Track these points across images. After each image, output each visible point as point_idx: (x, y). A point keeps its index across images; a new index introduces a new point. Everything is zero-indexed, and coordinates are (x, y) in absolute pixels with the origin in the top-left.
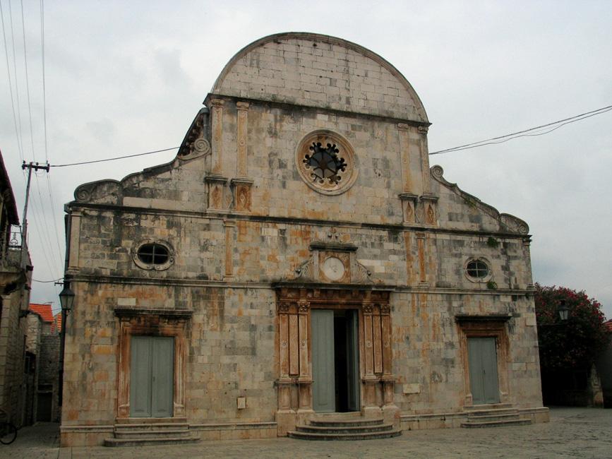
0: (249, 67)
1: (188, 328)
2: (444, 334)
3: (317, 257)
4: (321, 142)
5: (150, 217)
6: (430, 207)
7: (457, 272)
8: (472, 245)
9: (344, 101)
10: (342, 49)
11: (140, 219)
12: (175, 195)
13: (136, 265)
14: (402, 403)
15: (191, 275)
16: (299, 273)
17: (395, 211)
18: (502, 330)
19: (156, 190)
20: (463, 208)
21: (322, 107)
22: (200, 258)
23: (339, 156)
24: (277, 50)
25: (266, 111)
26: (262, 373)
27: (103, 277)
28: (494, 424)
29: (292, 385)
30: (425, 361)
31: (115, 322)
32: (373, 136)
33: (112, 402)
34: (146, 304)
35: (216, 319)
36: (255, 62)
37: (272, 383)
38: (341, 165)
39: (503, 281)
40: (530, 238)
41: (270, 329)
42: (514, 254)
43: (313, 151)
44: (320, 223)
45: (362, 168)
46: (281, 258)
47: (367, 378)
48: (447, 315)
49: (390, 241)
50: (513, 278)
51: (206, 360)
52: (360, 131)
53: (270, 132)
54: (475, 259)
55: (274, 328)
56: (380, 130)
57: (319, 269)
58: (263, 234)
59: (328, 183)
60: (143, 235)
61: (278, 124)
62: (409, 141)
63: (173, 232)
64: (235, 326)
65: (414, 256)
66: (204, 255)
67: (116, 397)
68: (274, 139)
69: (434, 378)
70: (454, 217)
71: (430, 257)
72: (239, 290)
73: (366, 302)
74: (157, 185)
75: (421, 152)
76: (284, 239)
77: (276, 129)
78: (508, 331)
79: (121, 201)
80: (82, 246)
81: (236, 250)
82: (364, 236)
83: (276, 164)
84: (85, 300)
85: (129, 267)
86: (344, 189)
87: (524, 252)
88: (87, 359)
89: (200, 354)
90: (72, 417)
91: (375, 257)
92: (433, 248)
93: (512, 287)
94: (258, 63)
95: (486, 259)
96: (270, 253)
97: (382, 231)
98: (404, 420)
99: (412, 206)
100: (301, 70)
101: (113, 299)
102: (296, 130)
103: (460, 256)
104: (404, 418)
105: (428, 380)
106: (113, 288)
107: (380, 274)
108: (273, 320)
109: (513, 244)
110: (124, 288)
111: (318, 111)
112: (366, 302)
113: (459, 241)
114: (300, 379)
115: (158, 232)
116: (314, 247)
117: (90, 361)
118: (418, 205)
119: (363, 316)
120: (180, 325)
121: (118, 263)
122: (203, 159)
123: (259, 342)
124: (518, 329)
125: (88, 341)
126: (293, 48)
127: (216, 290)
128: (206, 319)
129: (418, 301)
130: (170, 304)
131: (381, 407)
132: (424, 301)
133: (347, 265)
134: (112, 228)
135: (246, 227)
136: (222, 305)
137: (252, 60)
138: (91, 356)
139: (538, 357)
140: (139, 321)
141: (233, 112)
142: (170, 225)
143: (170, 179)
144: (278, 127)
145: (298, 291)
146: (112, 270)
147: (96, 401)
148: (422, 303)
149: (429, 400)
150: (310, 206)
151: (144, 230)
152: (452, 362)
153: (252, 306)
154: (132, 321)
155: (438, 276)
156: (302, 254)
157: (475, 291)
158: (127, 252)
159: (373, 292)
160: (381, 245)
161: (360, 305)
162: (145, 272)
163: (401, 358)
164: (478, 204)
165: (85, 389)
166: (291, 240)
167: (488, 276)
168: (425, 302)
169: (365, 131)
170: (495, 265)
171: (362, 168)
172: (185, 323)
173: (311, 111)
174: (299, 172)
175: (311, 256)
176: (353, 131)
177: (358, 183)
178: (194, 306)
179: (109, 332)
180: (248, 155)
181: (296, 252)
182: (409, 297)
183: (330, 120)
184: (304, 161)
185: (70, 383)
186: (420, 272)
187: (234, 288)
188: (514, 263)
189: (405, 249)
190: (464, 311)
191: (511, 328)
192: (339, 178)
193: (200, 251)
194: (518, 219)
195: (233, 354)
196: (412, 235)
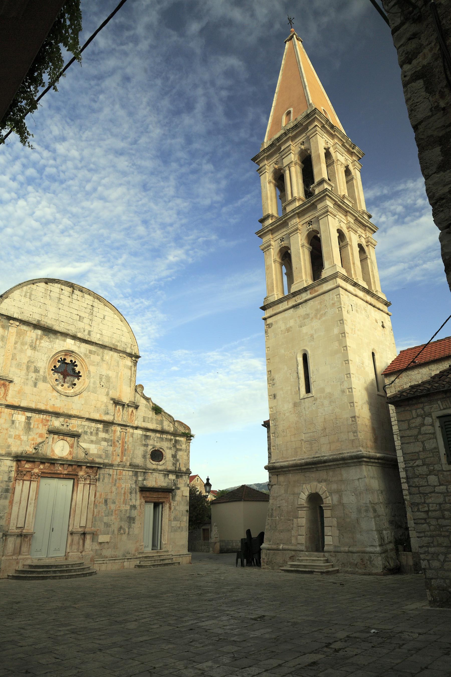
0: (23, 297)
3: (52, 439)
7: (144, 457)
9: (86, 333)
14: (96, 550)
18: (167, 498)
20: (153, 414)
23: (77, 369)
24: (46, 290)
25: (31, 331)
28: (157, 565)
29: (18, 536)
30: (116, 519)
32: (102, 360)
38: (78, 375)
39: (171, 465)
41: (7, 491)
42: (180, 448)
43: (60, 364)
44: (57, 415)
45: (92, 380)
46: (24, 438)
47: (74, 530)
48: (134, 486)
49: (103, 432)
52: (94, 354)
53: (31, 346)
54: (156, 449)
55: (11, 491)
56: (108, 355)
57: (52, 448)
58: (14, 419)
59: (67, 387)
65: (118, 444)
68: (34, 351)
69: (120, 531)
70: (146, 420)
82: (86, 427)
83: (32, 368)
86: (78, 392)
87: (186, 447)
91: (92, 442)
93: (177, 469)
94: (30, 296)
96: (17, 433)
98: (95, 562)
99: (121, 409)
100: (61, 306)
102: (50, 347)
103: (146, 445)
104: (97, 561)
105: (116, 532)
107: (93, 454)
111: (68, 337)
112: (81, 473)
114: (24, 531)
116: (51, 432)
118: (125, 409)
119: (78, 483)
124: (178, 498)
126: (58, 290)
131: (81, 552)
133: (72, 447)
137: (26, 292)
139: (188, 517)
144: (38, 343)
149: (115, 547)
150: (52, 402)
156: (41, 436)
157: (154, 470)
160: (97, 434)
161: (77, 475)
163: (100, 516)
166: (34, 424)
167: (163, 460)
168: (121, 476)
170: (168, 454)
171: (92, 380)
175: (47, 438)
176: (89, 354)
177: (87, 389)
180: (12, 359)
181: (37, 434)
182: (111, 472)
184: (52, 370)
186: (120, 455)
188: (180, 453)
189: (112, 438)
190: (145, 483)
191: (174, 497)
194: (185, 425)
196: (118, 429)
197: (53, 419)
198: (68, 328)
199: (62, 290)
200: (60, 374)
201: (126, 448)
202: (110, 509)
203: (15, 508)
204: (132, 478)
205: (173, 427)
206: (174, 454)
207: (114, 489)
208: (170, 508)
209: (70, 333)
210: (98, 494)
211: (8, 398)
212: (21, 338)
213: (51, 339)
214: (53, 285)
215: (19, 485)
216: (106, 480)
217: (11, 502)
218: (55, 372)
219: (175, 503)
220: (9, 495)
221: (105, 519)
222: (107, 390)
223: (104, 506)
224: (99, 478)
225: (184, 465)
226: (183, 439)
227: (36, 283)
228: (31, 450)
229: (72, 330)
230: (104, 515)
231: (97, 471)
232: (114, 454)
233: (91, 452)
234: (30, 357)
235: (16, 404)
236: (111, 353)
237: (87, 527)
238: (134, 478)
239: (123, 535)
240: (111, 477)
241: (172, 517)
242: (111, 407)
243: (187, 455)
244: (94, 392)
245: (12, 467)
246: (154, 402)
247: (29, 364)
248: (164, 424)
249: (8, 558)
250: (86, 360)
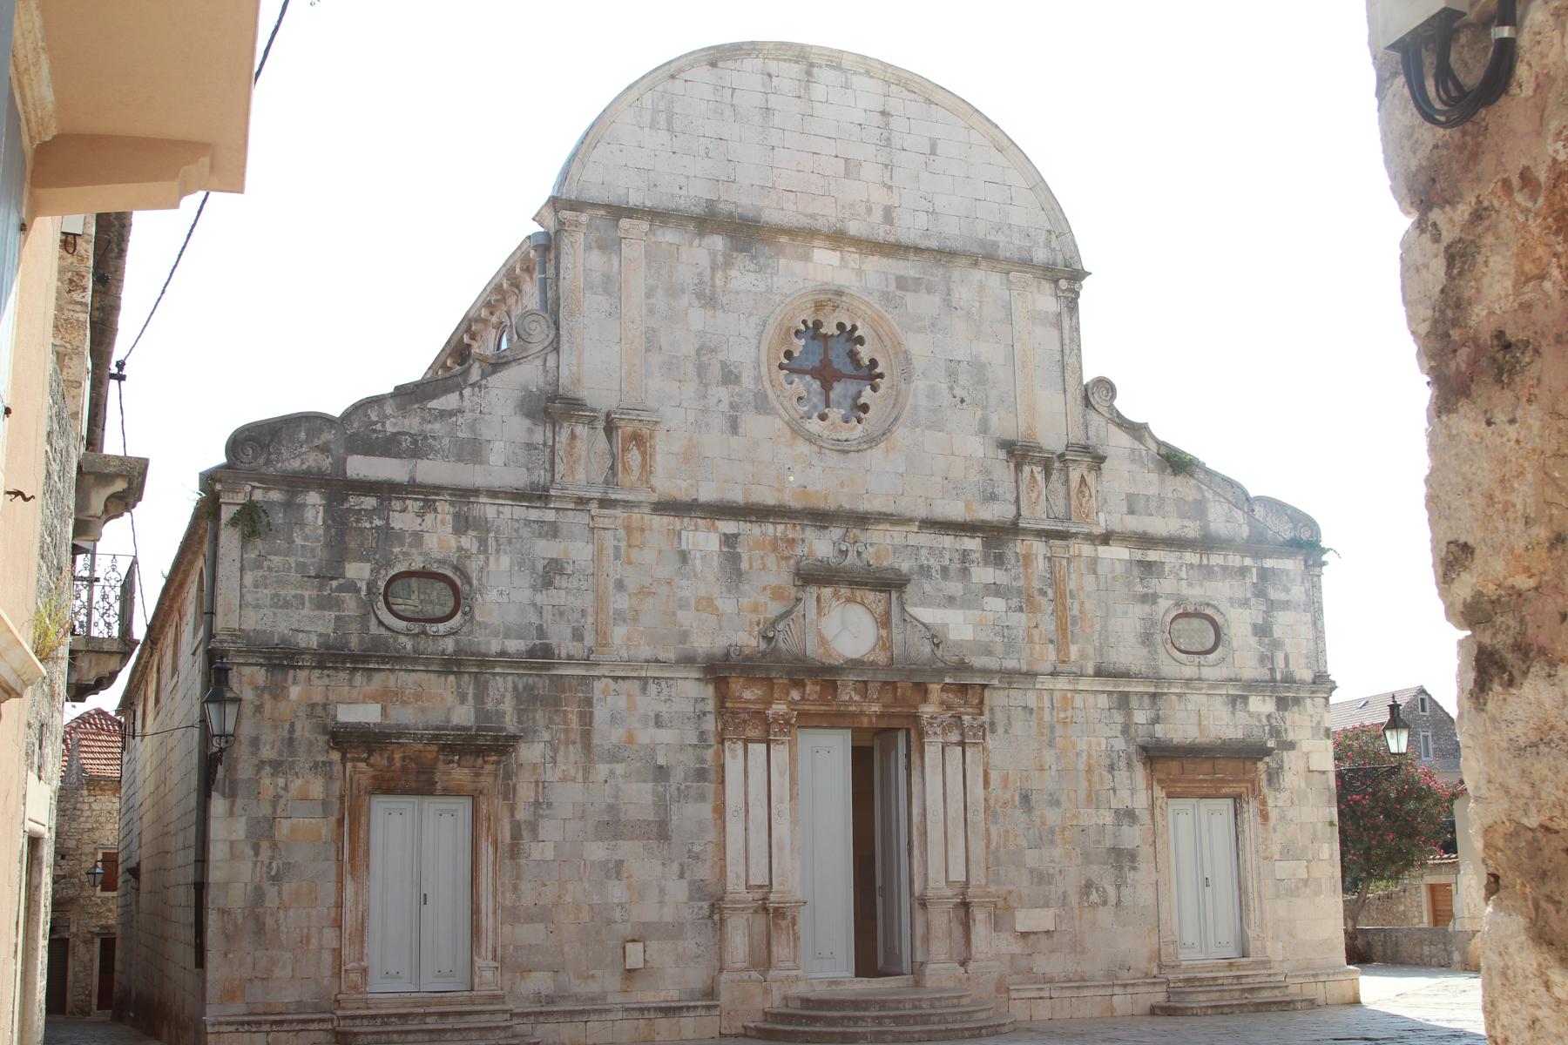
0: (647, 130)
1: (508, 776)
2: (1114, 790)
4: (821, 318)
5: (414, 506)
7: (1146, 639)
8: (1183, 574)
11: (389, 509)
12: (472, 451)
13: (381, 623)
14: (1013, 956)
15: (514, 645)
16: (770, 640)
17: (999, 491)
19: (426, 438)
22: (535, 605)
23: (865, 353)
25: (690, 244)
26: (684, 883)
27: (301, 652)
31: (331, 763)
32: (948, 303)
33: (327, 957)
34: (404, 716)
35: (575, 752)
37: (706, 905)
39: (1254, 662)
40: (1324, 558)
41: (701, 775)
42: (1283, 596)
43: (803, 342)
44: (821, 518)
46: (727, 605)
48: (1120, 744)
49: (986, 564)
50: (1280, 657)
51: (549, 853)
52: (916, 291)
53: (699, 296)
54: (1191, 609)
57: (819, 632)
58: (684, 547)
59: (838, 421)
60: (396, 550)
61: (719, 275)
63: (469, 542)
64: (620, 769)
65: (1043, 601)
66: (540, 599)
67: (335, 945)
69: (1088, 894)
71: (1082, 604)
72: (628, 682)
73: (928, 710)
74: (428, 427)
77: (713, 286)
78: (1264, 783)
79: (340, 464)
80: (249, 578)
81: (620, 585)
82: (924, 552)
83: (715, 371)
84: (259, 709)
85: (365, 628)
87: (1307, 592)
88: (265, 852)
89: (535, 838)
90: (230, 995)
91: (951, 601)
92: (1089, 581)
93: (1278, 677)
96: (702, 593)
99: (1040, 477)
101: (325, 706)
102: (762, 288)
103: (1149, 599)
105: (1074, 899)
106: (326, 681)
108: (709, 754)
110: (350, 680)
112: (928, 710)
115: (431, 542)
117: (273, 858)
118: (1055, 475)
120: (489, 768)
121: (338, 618)
122: (539, 362)
123: (674, 807)
124: (1290, 780)
125: (266, 810)
127: (574, 682)
128: (549, 753)
130: (463, 715)
133: (884, 622)
134: (321, 531)
135: (642, 530)
136: (587, 718)
137: (655, 111)
138: (274, 846)
139: (1337, 846)
140: (391, 760)
141: (608, 246)
142: (462, 524)
143: (461, 411)
144: (719, 282)
146: (320, 635)
147: (289, 955)
148: (1062, 715)
149: (1077, 947)
151: (399, 536)
152: (1132, 856)
153: (658, 721)
154: (372, 760)
155: (1099, 651)
156: (777, 594)
157: (1188, 682)
158: (358, 591)
160: (965, 572)
161: (916, 718)
162: (402, 639)
165: (260, 928)
166: (750, 558)
167: (1220, 649)
168: (1069, 713)
170: (1239, 624)
172: (498, 763)
174: (771, 395)
178: (520, 722)
179: (317, 788)
180: (648, 350)
182: (1031, 699)
183: (844, 264)
184: (781, 367)
185: (224, 912)
187: (615, 678)
189: (1021, 583)
190: (1160, 731)
191: (1274, 776)
192: (865, 408)
193: (533, 587)
195: (615, 837)
196: (1039, 547)
197: (810, 534)
198: (810, 210)
199: (770, 76)
200: (808, 378)
201: (1076, 612)
203: (734, 828)
204: (1111, 716)
205: (1249, 524)
206: (1260, 621)
208: (1265, 817)
209: (820, 224)
210: (995, 778)
211: (656, 481)
213: (762, 260)
214: (737, 65)
215: (734, 757)
216: (1018, 728)
217: (720, 810)
218: (792, 371)
220: (710, 787)
221: (1032, 858)
222: (979, 414)
223: (1019, 815)
224: (992, 724)
225: (1303, 662)
226: (1291, 565)
227: (681, 71)
228: (754, 643)
229: (826, 213)
230: (1025, 844)
231: (982, 702)
232: (1036, 638)
233: (953, 636)
234: (701, 334)
235: (684, 497)
236: (978, 275)
237: (973, 882)
238: (1119, 717)
240: (1034, 717)
241: (1276, 849)
242: (1003, 474)
243: (1315, 624)
245: (703, 699)
246: (1161, 438)
247: (704, 359)
248: (1211, 517)
249: (736, 976)
250: (889, 317)
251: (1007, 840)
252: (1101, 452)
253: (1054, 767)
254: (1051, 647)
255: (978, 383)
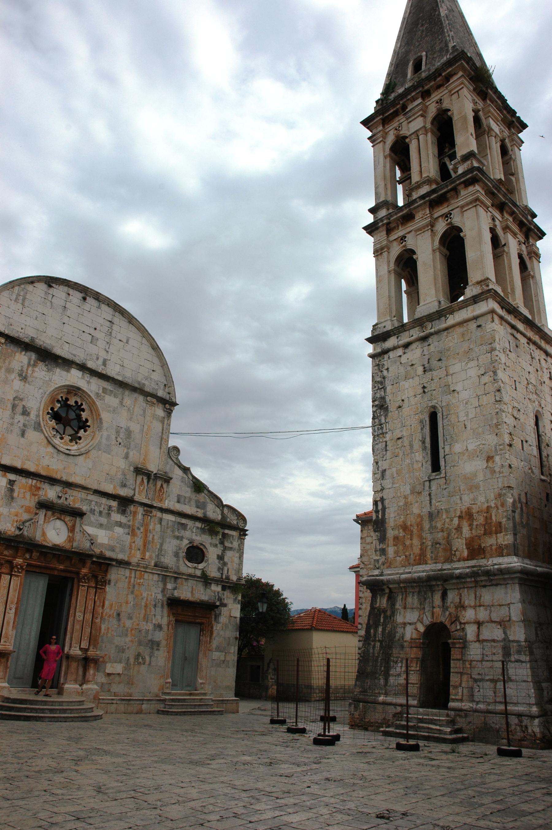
0: (13, 301)
3: (43, 517)
4: (69, 397)
6: (162, 486)
7: (176, 555)
9: (100, 362)
10: (110, 310)
14: (102, 684)
16: (20, 529)
18: (208, 618)
21: (78, 362)
23: (84, 415)
24: (46, 293)
25: (21, 352)
30: (132, 641)
32: (121, 403)
36: (21, 298)
38: (84, 425)
39: (216, 570)
40: (247, 533)
42: (230, 545)
43: (59, 405)
44: (52, 481)
45: (105, 434)
47: (72, 652)
48: (160, 596)
52: (110, 395)
53: (20, 375)
54: (195, 544)
56: (129, 399)
57: (43, 530)
59: (68, 441)
61: (30, 369)
62: (154, 416)
65: (138, 532)
68: (23, 383)
69: (138, 659)
73: (84, 571)
75: (163, 430)
76: (12, 490)
77: (27, 372)
78: (213, 619)
82: (93, 503)
83: (19, 409)
86: (83, 450)
87: (239, 545)
91: (101, 526)
93: (224, 577)
94: (24, 300)
95: (205, 546)
97: (111, 501)
98: (101, 701)
99: (145, 481)
100: (66, 320)
102: (47, 379)
103: (180, 538)
104: (103, 699)
105: (132, 660)
107: (102, 545)
109: (231, 535)
111: (74, 366)
113: (183, 524)
119: (79, 586)
124: (223, 619)
126: (64, 295)
129: (135, 578)
132: (140, 579)
133: (72, 530)
137: (18, 295)
144: (30, 372)
145: (16, 549)
148: (139, 581)
149: (130, 683)
150: (46, 462)
152: (158, 644)
155: (158, 556)
157: (190, 575)
159: (93, 562)
160: (109, 515)
161: (78, 573)
163: (109, 635)
164: (207, 493)
166: (19, 492)
167: (204, 563)
168: (142, 581)
169: (115, 397)
170: (212, 553)
171: (105, 434)
173: (66, 363)
174: (42, 425)
175: (36, 514)
176: (103, 394)
177: (98, 447)
181: (22, 507)
182: (127, 572)
183: (83, 378)
184: (48, 413)
186: (141, 548)
189: (131, 523)
190: (176, 594)
191: (217, 617)
192: (80, 438)
194: (239, 513)
196: (140, 510)
198: (74, 352)
199: (69, 294)
202: (124, 627)
207: (131, 598)
212: (7, 361)
219: (219, 626)
222: (126, 451)
223: (115, 622)
225: (234, 572)
229: (79, 357)
232: (133, 547)
233: (100, 541)
239: (142, 666)
242: (131, 476)
243: (240, 558)
244: (108, 451)
247: (16, 402)
250: (97, 403)
251: (108, 632)
252: (170, 475)
253: (132, 603)
254: (138, 551)
255: (127, 438)
